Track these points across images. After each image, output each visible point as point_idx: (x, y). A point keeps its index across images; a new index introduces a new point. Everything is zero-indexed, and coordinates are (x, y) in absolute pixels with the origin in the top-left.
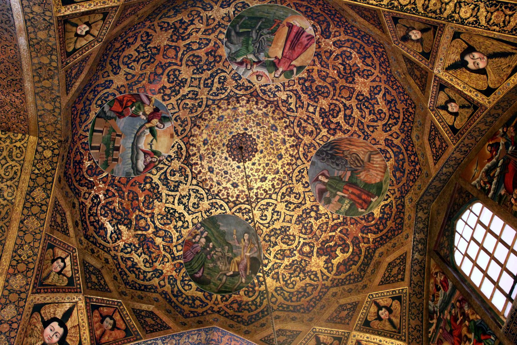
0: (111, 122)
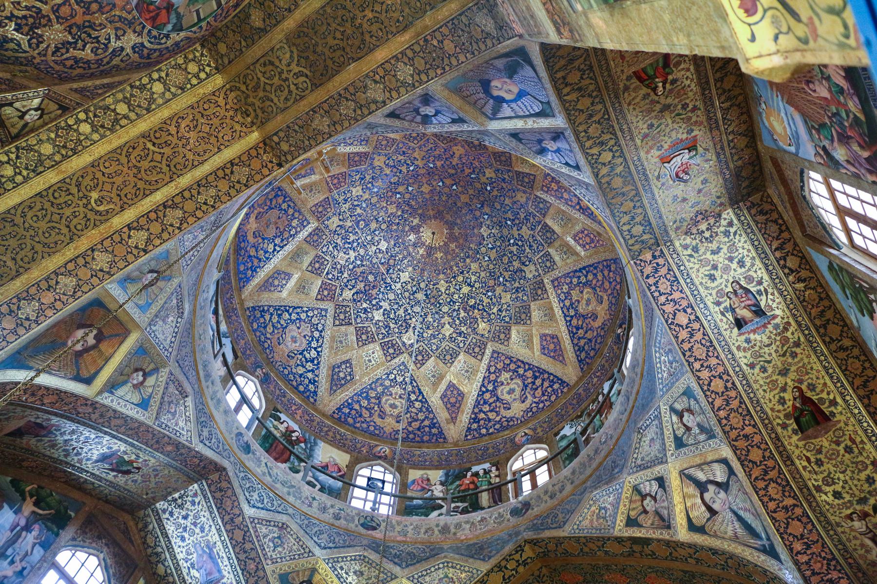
0: (181, 11)
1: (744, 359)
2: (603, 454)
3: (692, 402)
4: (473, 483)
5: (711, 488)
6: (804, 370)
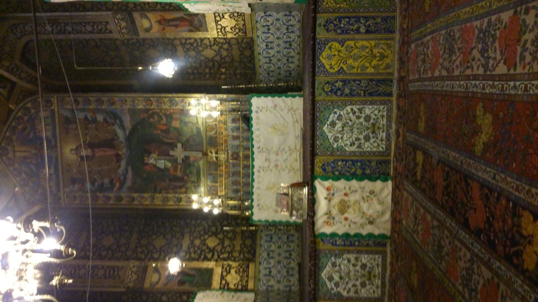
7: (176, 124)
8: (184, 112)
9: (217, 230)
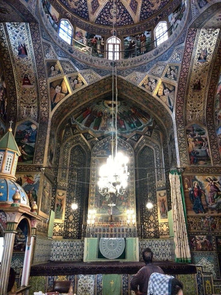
1: (194, 67)
2: (143, 63)
3: (176, 70)
4: (95, 41)
5: (167, 89)
6: (204, 77)
7: (124, 204)
8: (128, 207)
9: (76, 220)
